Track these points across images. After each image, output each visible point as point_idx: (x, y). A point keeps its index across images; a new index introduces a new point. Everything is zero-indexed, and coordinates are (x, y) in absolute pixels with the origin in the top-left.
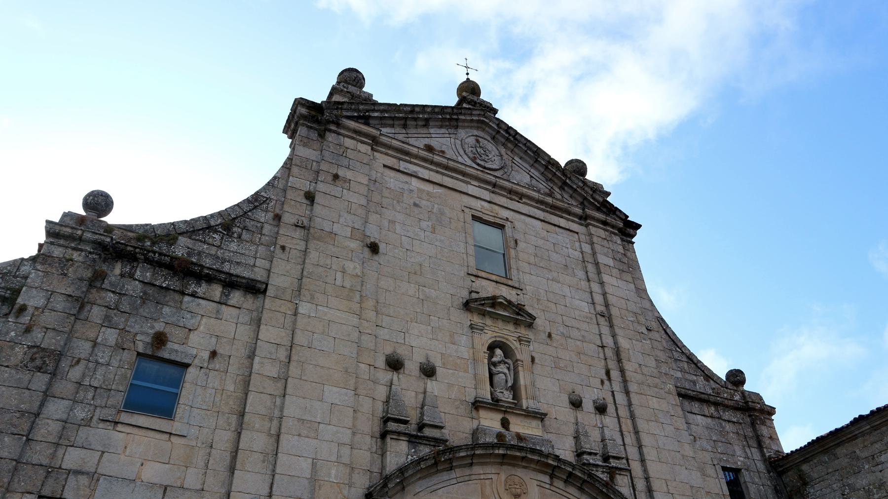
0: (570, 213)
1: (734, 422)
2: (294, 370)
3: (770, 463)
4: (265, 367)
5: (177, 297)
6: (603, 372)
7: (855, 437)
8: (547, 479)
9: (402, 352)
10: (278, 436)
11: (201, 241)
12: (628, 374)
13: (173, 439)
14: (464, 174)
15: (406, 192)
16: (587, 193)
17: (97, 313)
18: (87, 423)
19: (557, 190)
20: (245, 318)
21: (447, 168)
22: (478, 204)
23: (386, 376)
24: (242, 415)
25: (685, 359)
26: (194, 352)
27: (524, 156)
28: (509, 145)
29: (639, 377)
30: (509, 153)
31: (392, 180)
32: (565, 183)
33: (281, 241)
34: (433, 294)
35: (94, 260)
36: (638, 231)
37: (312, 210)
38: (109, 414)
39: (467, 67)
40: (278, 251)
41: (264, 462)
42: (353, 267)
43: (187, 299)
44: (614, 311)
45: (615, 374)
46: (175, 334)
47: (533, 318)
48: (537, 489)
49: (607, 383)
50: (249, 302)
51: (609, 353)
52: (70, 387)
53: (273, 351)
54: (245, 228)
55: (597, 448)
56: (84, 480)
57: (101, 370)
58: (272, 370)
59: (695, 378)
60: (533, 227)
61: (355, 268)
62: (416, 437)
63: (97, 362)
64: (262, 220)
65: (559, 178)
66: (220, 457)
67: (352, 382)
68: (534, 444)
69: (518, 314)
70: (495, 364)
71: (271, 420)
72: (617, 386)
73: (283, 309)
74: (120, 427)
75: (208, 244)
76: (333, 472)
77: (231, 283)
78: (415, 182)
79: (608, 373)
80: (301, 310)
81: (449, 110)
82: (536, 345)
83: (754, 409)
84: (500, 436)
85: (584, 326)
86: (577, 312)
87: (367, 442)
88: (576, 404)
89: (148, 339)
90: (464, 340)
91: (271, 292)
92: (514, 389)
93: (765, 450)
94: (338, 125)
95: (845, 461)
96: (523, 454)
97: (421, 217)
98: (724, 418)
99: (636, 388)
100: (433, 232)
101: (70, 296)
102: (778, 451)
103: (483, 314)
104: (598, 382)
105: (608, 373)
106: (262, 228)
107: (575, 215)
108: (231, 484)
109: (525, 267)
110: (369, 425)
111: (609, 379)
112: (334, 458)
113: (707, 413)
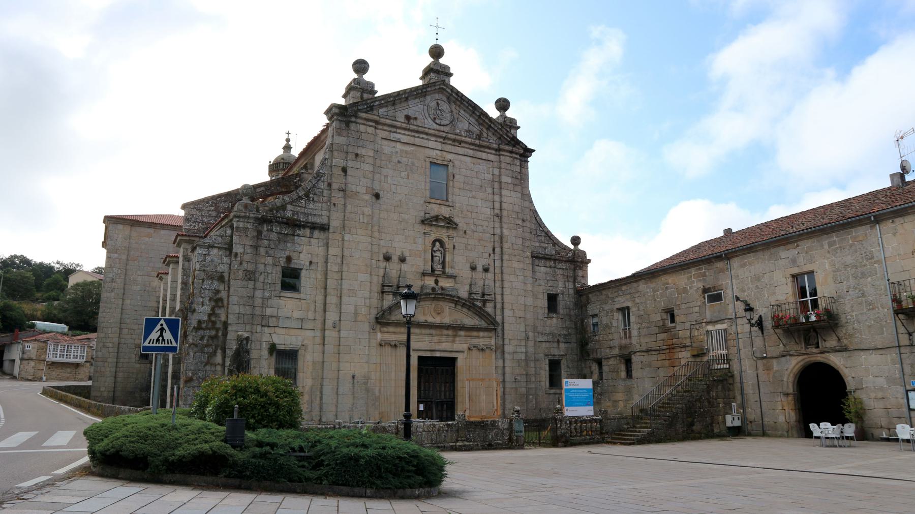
0: (490, 148)
1: (563, 269)
2: (345, 268)
3: (577, 291)
4: (333, 267)
5: (292, 237)
6: (491, 249)
7: (610, 288)
8: (453, 305)
9: (391, 251)
10: (341, 296)
11: (297, 206)
12: (505, 250)
13: (302, 301)
14: (427, 134)
15: (394, 154)
16: (503, 132)
17: (262, 251)
18: (270, 298)
19: (485, 130)
20: (321, 244)
21: (417, 132)
22: (433, 153)
23: (383, 264)
24: (326, 288)
25: (544, 234)
26: (303, 263)
27: (466, 109)
28: (458, 103)
29: (510, 251)
30: (457, 108)
31: (386, 147)
32: (490, 126)
33: (333, 201)
34: (406, 217)
35: (256, 227)
36: (533, 153)
37: (346, 179)
38: (277, 293)
39: (437, 27)
40: (332, 206)
41: (336, 307)
42: (368, 211)
43: (296, 238)
44: (505, 213)
45: (498, 250)
46: (294, 255)
47: (457, 225)
48: (448, 310)
49: (492, 255)
50: (322, 235)
51: (497, 238)
52: (261, 284)
53: (335, 259)
54: (315, 194)
55: (480, 290)
56: (274, 319)
57: (270, 276)
58: (336, 268)
59: (547, 245)
60: (465, 163)
61: (369, 211)
62: (396, 293)
63: (267, 272)
64: (322, 187)
65: (487, 124)
66: (320, 306)
67: (369, 270)
68: (449, 291)
69: (449, 223)
70: (435, 252)
71: (337, 290)
72: (497, 257)
73: (337, 238)
74: (282, 298)
75: (300, 207)
76: (363, 310)
77: (314, 227)
78: (399, 146)
79: (494, 250)
80: (345, 238)
81: (421, 87)
82: (457, 238)
83: (578, 262)
84: (433, 289)
85: (486, 223)
86: (483, 215)
87: (376, 295)
88: (473, 268)
89: (284, 260)
90: (420, 241)
91: (331, 230)
92: (444, 263)
93: (576, 284)
94: (356, 117)
95: (603, 297)
96: (443, 296)
97: (402, 169)
98: (558, 267)
99: (507, 257)
100: (408, 178)
101: (251, 245)
102: (584, 284)
103: (431, 225)
104: (488, 255)
105: (494, 250)
106: (323, 192)
107: (493, 149)
108: (325, 316)
109: (456, 191)
110: (376, 288)
111: (494, 253)
112: (363, 304)
113: (548, 265)
